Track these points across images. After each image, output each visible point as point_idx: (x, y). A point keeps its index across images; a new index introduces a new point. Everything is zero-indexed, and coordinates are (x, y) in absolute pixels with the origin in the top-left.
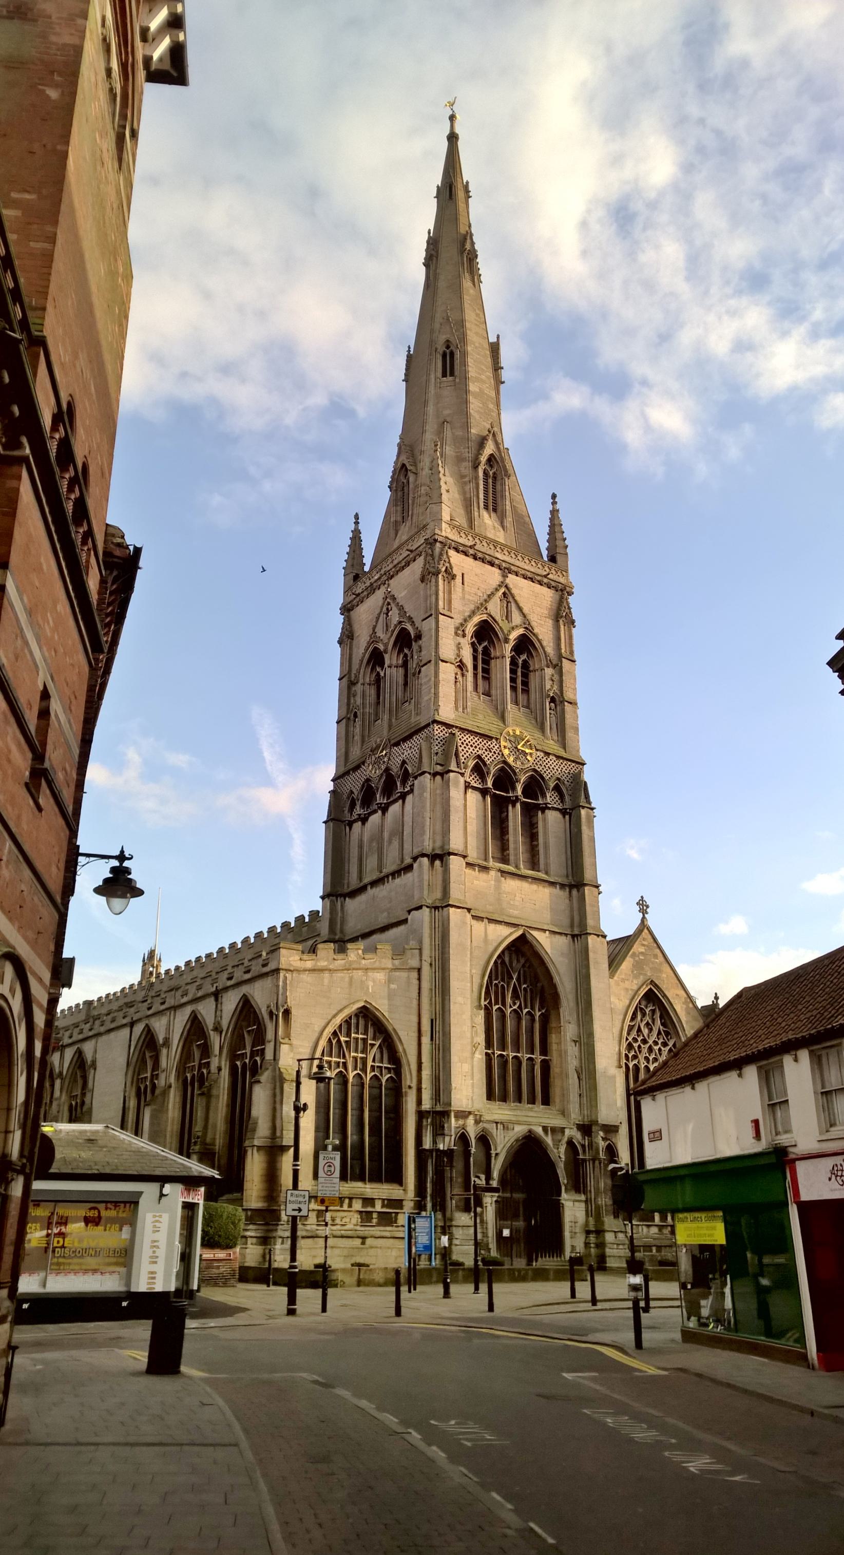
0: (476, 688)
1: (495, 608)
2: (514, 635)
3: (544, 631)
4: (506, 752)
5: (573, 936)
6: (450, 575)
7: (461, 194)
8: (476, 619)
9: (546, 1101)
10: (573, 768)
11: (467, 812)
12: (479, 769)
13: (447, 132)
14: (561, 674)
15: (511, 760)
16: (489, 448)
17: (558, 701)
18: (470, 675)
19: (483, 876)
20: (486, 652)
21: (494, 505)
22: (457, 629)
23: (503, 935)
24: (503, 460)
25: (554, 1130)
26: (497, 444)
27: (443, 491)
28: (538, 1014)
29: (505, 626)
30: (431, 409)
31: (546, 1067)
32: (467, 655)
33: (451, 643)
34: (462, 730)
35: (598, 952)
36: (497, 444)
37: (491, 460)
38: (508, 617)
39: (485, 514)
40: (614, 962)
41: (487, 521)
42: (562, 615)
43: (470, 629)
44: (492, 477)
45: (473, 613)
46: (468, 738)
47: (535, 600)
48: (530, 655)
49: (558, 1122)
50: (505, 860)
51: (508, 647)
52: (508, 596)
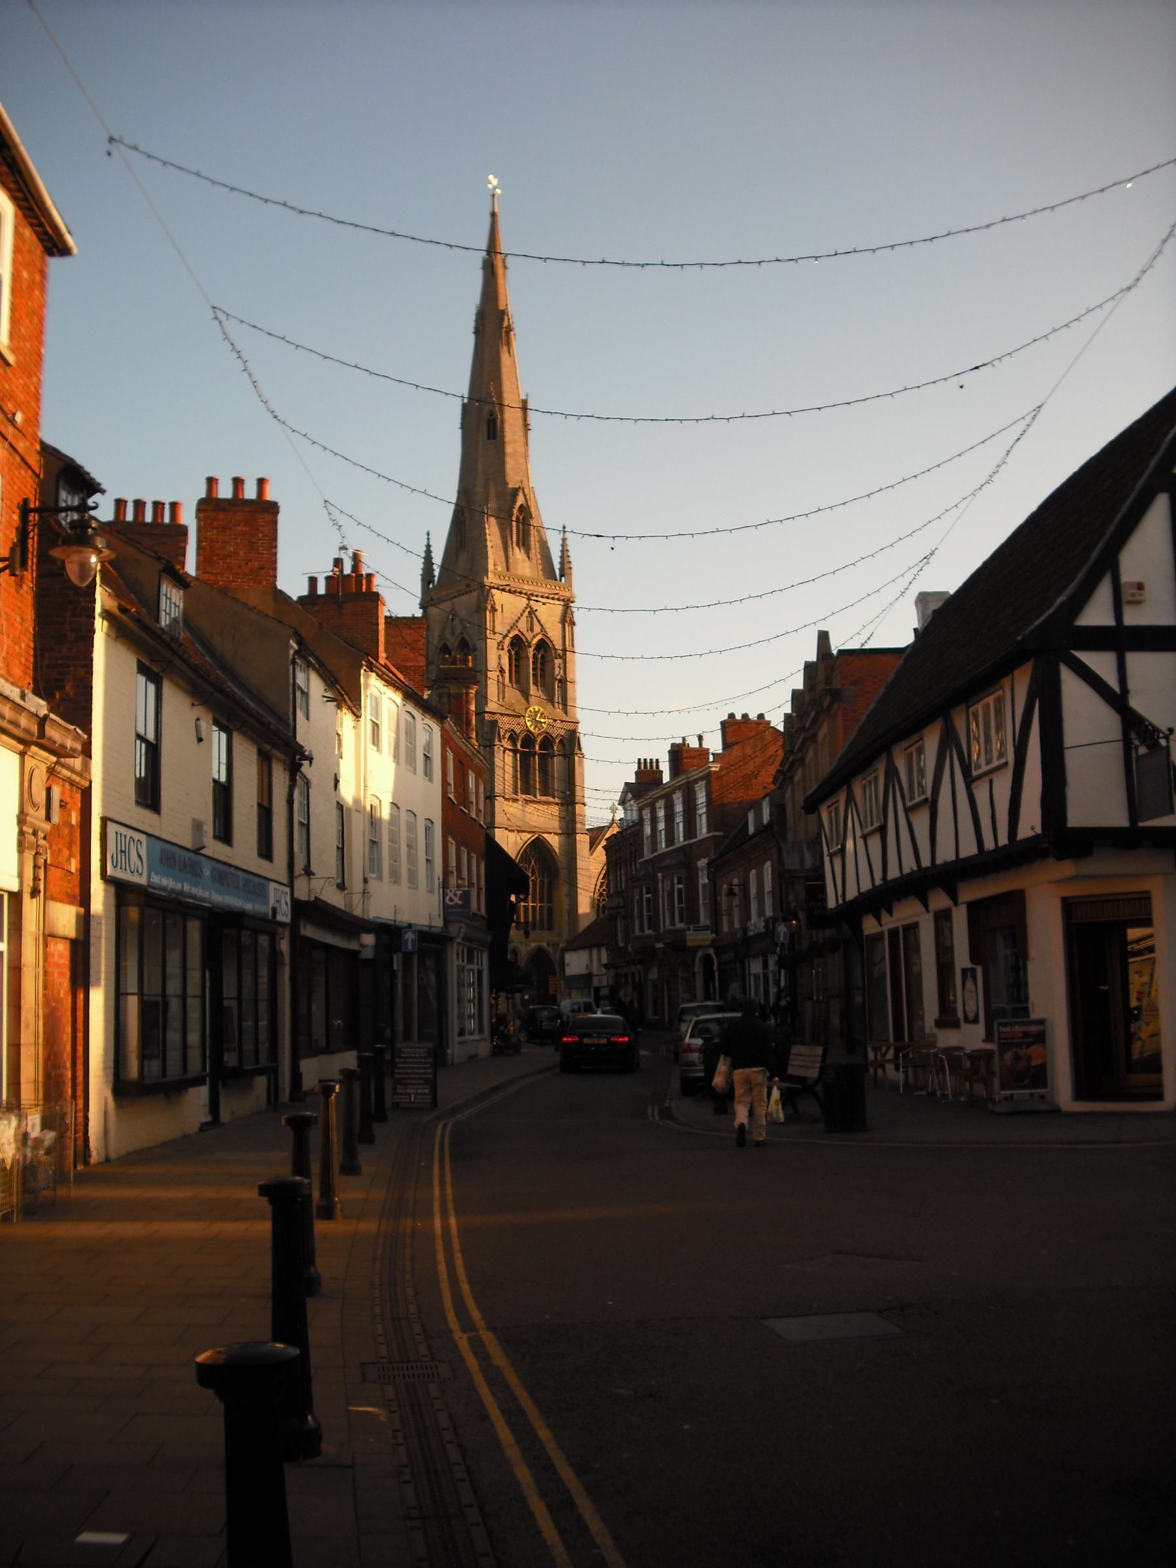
0: (510, 681)
1: (523, 625)
2: (535, 641)
3: (555, 634)
4: (529, 724)
5: (568, 834)
6: (494, 610)
7: (500, 271)
8: (511, 635)
9: (550, 928)
10: (570, 727)
11: (505, 764)
12: (513, 738)
13: (489, 210)
14: (565, 662)
15: (532, 729)
16: (520, 500)
17: (563, 682)
18: (507, 674)
19: (515, 805)
20: (516, 653)
21: (524, 543)
22: (499, 644)
23: (526, 837)
24: (528, 507)
25: (553, 945)
26: (525, 496)
27: (489, 549)
28: (546, 881)
29: (529, 635)
30: (480, 466)
31: (550, 910)
32: (505, 662)
33: (496, 657)
34: (502, 714)
35: (582, 841)
36: (525, 496)
37: (521, 506)
38: (532, 630)
39: (516, 549)
40: (593, 845)
41: (518, 554)
42: (567, 620)
43: (507, 641)
44: (521, 523)
45: (509, 632)
46: (506, 719)
47: (549, 613)
48: (545, 651)
49: (556, 939)
50: (526, 791)
51: (531, 652)
52: (532, 613)
